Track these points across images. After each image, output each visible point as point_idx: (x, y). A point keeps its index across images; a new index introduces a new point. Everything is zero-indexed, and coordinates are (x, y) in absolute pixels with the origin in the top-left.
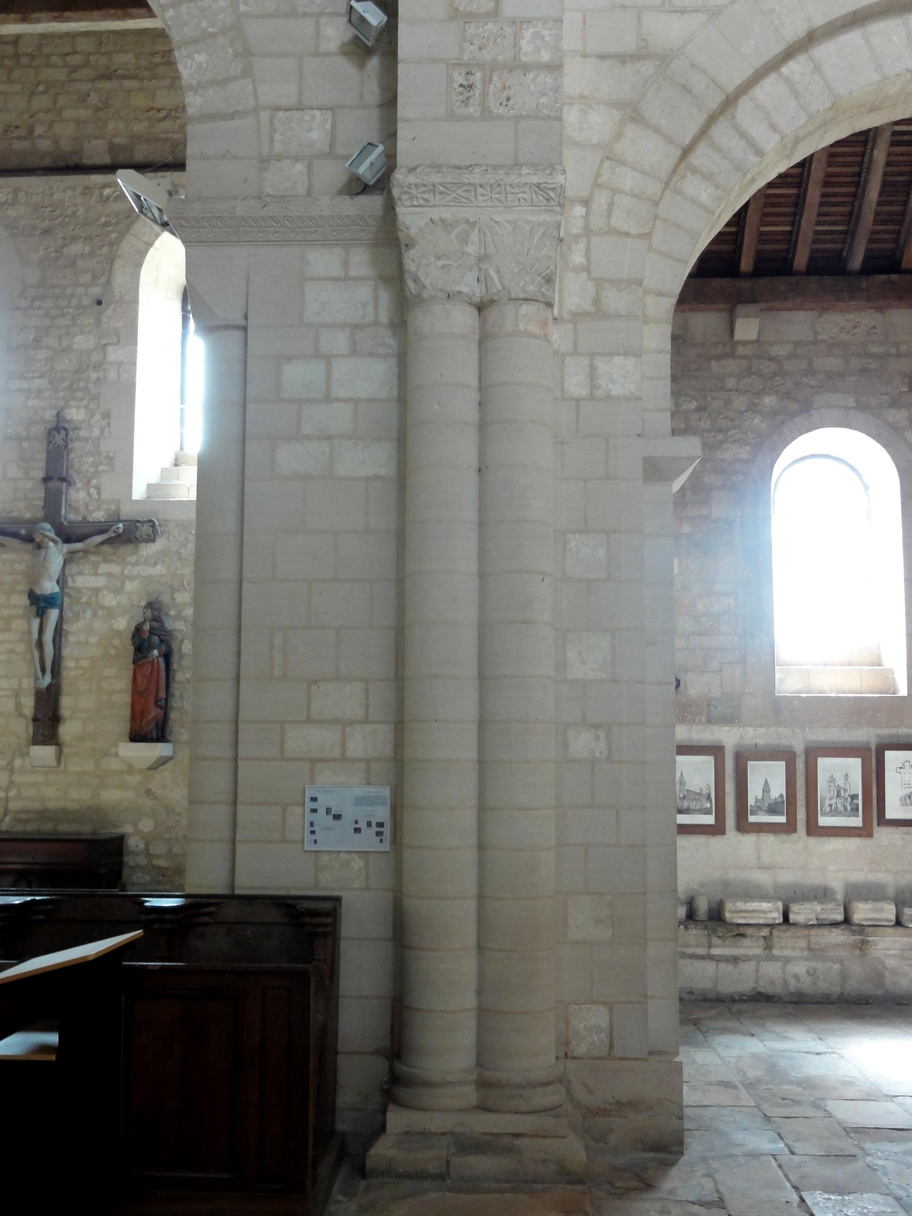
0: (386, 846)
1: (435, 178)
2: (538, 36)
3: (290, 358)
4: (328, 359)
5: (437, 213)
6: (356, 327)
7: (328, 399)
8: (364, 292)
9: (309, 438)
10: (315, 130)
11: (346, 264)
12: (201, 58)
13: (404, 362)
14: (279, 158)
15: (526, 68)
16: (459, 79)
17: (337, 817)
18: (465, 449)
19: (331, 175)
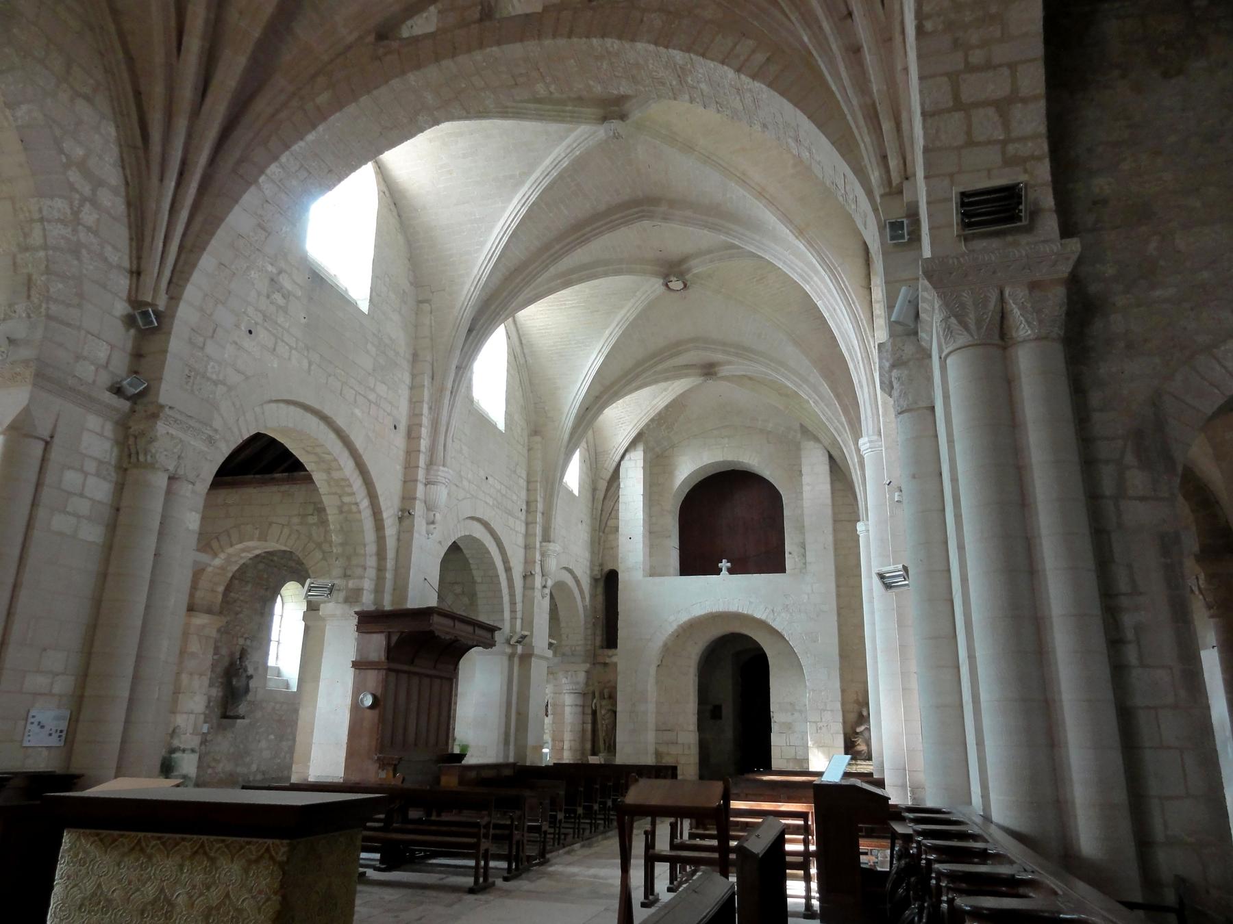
0: (62, 744)
1: (178, 416)
2: (213, 367)
3: (70, 468)
4: (86, 474)
5: (172, 431)
6: (101, 462)
7: (81, 495)
8: (107, 445)
9: (69, 513)
10: (102, 353)
11: (103, 427)
12: (60, 286)
13: (120, 488)
14: (85, 358)
15: (209, 379)
16: (187, 372)
17: (42, 727)
18: (151, 541)
19: (104, 379)
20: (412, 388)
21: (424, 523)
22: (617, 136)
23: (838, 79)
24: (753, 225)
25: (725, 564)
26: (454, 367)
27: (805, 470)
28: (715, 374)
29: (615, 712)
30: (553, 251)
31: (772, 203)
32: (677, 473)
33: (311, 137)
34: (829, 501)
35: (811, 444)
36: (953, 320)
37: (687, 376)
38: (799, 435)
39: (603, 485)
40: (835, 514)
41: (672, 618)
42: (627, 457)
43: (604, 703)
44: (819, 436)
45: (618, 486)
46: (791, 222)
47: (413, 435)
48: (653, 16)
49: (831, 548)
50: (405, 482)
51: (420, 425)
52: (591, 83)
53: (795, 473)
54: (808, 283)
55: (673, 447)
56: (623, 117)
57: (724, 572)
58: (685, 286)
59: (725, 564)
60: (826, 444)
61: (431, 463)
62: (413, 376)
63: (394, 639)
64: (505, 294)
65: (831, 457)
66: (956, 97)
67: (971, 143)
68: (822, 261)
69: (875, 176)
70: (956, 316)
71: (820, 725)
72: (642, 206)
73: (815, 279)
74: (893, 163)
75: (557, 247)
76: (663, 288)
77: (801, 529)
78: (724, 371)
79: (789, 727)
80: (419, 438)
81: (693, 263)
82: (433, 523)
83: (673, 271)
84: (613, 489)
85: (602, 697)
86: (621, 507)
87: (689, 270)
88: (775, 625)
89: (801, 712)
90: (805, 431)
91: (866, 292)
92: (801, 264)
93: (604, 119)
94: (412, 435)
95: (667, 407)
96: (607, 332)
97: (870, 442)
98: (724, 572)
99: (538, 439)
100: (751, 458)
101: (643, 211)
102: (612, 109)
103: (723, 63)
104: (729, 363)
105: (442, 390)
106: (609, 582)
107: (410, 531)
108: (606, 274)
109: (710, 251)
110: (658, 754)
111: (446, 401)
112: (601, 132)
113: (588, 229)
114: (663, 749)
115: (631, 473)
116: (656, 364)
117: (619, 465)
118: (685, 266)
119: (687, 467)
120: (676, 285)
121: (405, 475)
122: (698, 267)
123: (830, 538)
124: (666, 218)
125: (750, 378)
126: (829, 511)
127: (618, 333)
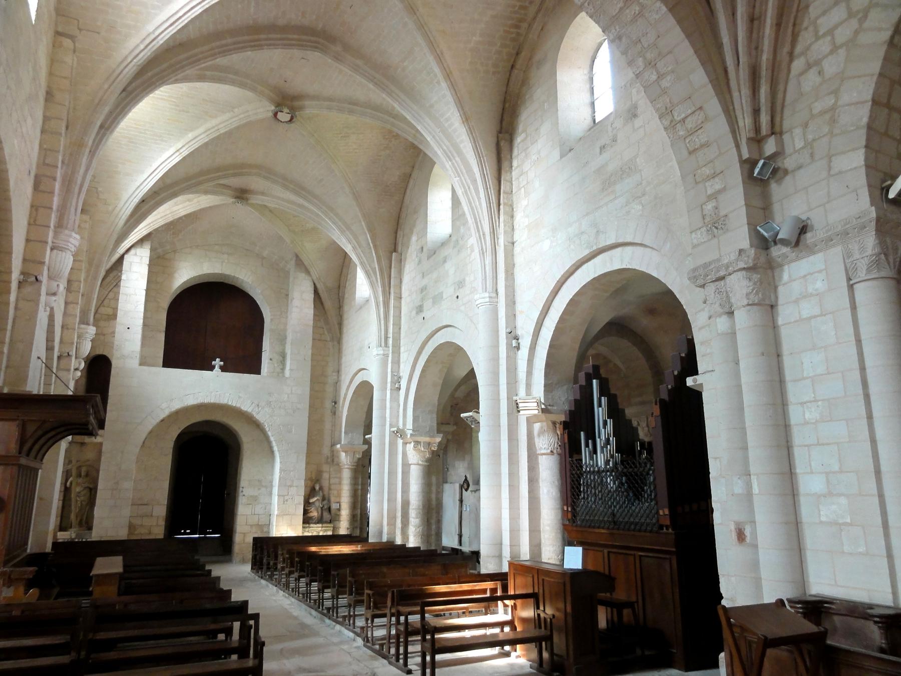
23: (732, 34)
24: (411, 93)
25: (218, 362)
26: (99, 124)
28: (247, 199)
29: (92, 491)
30: (224, 42)
31: (453, 86)
32: (176, 275)
35: (302, 276)
36: (883, 256)
37: (222, 194)
41: (164, 405)
42: (133, 251)
43: (80, 480)
44: (311, 270)
45: (118, 280)
46: (463, 109)
47: (42, 187)
49: (310, 359)
51: (55, 179)
53: (283, 297)
55: (175, 251)
57: (217, 368)
58: (291, 120)
59: (218, 362)
60: (315, 278)
62: (46, 119)
63: (31, 428)
64: (165, 65)
66: (889, 99)
67: (886, 134)
69: (745, 122)
70: (886, 255)
71: (286, 498)
72: (316, 37)
73: (457, 159)
74: (764, 119)
75: (230, 41)
76: (271, 114)
77: (282, 340)
78: (256, 200)
79: (255, 499)
81: (307, 103)
82: (54, 294)
83: (287, 103)
85: (79, 475)
86: (121, 298)
87: (301, 108)
88: (260, 417)
89: (266, 487)
90: (300, 264)
91: (496, 182)
92: (448, 143)
95: (185, 216)
96: (190, 135)
97: (490, 297)
98: (217, 368)
99: (86, 217)
101: (318, 43)
104: (263, 194)
105: (80, 145)
106: (99, 369)
108: (233, 83)
109: (330, 99)
110: (131, 527)
111: (84, 160)
113: (263, 36)
114: (137, 522)
115: (135, 268)
116: (219, 178)
117: (122, 258)
118: (296, 104)
119: (185, 273)
120: (284, 116)
122: (310, 109)
123: (310, 352)
124: (337, 58)
125: (270, 211)
126: (310, 330)
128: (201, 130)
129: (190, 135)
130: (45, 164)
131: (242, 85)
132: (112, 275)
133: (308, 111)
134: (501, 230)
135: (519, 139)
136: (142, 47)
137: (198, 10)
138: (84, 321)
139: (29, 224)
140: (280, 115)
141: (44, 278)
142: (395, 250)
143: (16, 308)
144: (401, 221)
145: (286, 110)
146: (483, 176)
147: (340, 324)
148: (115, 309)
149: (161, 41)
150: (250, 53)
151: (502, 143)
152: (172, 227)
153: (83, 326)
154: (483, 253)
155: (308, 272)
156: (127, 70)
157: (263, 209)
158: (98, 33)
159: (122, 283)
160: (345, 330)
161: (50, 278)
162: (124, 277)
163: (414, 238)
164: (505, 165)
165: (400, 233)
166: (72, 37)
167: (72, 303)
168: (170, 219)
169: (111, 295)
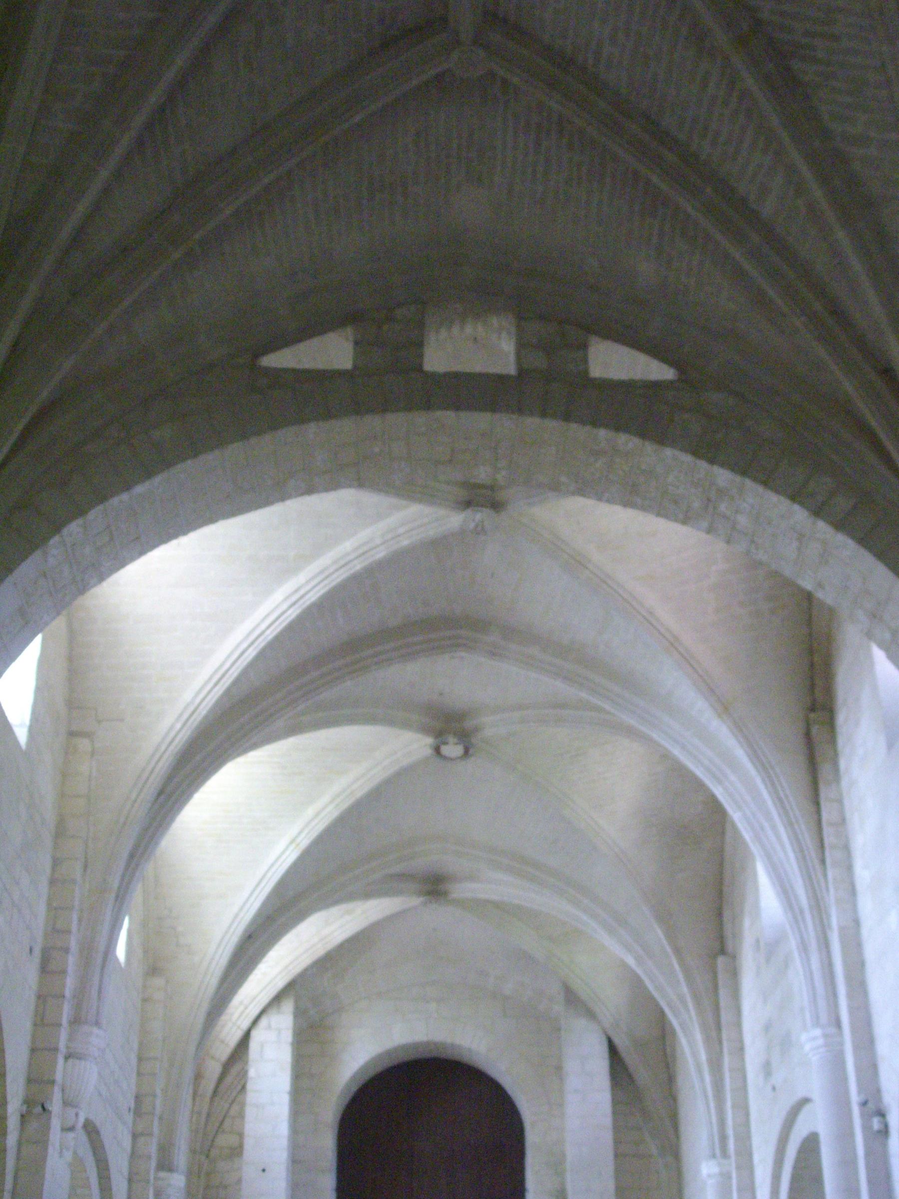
20: (53, 882)
21: (58, 1128)
22: (480, 530)
27: (571, 1066)
31: (687, 660)
33: (139, 489)
34: (608, 1121)
35: (581, 1023)
38: (558, 1007)
39: (213, 1069)
40: (617, 1142)
42: (264, 1022)
45: (244, 1074)
48: (686, 416)
50: (33, 1050)
51: (67, 950)
52: (563, 479)
54: (719, 782)
56: (496, 506)
58: (466, 752)
61: (76, 1021)
62: (56, 863)
65: (613, 1050)
68: (755, 756)
73: (733, 778)
75: (315, 674)
76: (429, 751)
77: (557, 1165)
78: (462, 890)
80: (64, 972)
83: (451, 728)
84: (229, 1079)
86: (250, 1113)
87: (476, 730)
90: (572, 998)
93: (468, 504)
94: (48, 967)
96: (310, 812)
99: (158, 982)
100: (474, 1038)
102: (481, 497)
103: (793, 498)
104: (472, 878)
107: (42, 1142)
108: (351, 720)
112: (455, 520)
115: (270, 1052)
120: (453, 749)
121: (34, 1038)
123: (611, 1185)
126: (608, 1137)
127: (331, 814)
128: (326, 799)
129: (310, 812)
130: (55, 930)
131: (371, 720)
132: (234, 1071)
133: (488, 732)
134: (831, 898)
135: (841, 718)
136: (179, 726)
137: (251, 653)
138: (166, 1165)
139: (35, 1025)
140: (446, 750)
141: (55, 1106)
142: (723, 951)
143: (18, 1158)
144: (725, 889)
145: (452, 739)
146: (780, 801)
147: (674, 1119)
148: (241, 1135)
149: (203, 711)
150: (349, 683)
151: (814, 730)
152: (330, 963)
153: (162, 1174)
154: (804, 947)
155: (591, 1015)
156: (160, 764)
157: (480, 907)
158: (122, 720)
159: (249, 1086)
160: (682, 1128)
161: (66, 1103)
162: (252, 1073)
163: (747, 923)
164: (825, 770)
165: (727, 914)
166: (88, 735)
167: (142, 1134)
168: (320, 951)
169: (235, 1108)
